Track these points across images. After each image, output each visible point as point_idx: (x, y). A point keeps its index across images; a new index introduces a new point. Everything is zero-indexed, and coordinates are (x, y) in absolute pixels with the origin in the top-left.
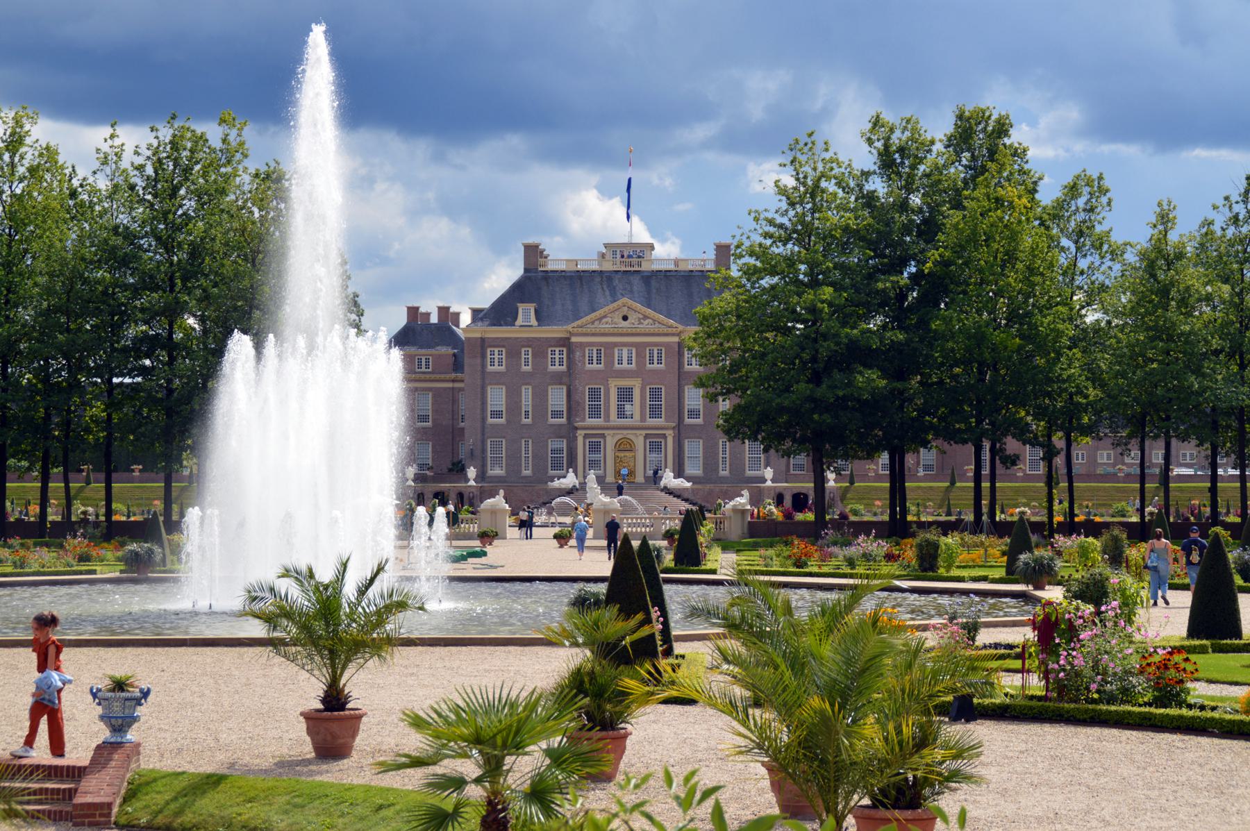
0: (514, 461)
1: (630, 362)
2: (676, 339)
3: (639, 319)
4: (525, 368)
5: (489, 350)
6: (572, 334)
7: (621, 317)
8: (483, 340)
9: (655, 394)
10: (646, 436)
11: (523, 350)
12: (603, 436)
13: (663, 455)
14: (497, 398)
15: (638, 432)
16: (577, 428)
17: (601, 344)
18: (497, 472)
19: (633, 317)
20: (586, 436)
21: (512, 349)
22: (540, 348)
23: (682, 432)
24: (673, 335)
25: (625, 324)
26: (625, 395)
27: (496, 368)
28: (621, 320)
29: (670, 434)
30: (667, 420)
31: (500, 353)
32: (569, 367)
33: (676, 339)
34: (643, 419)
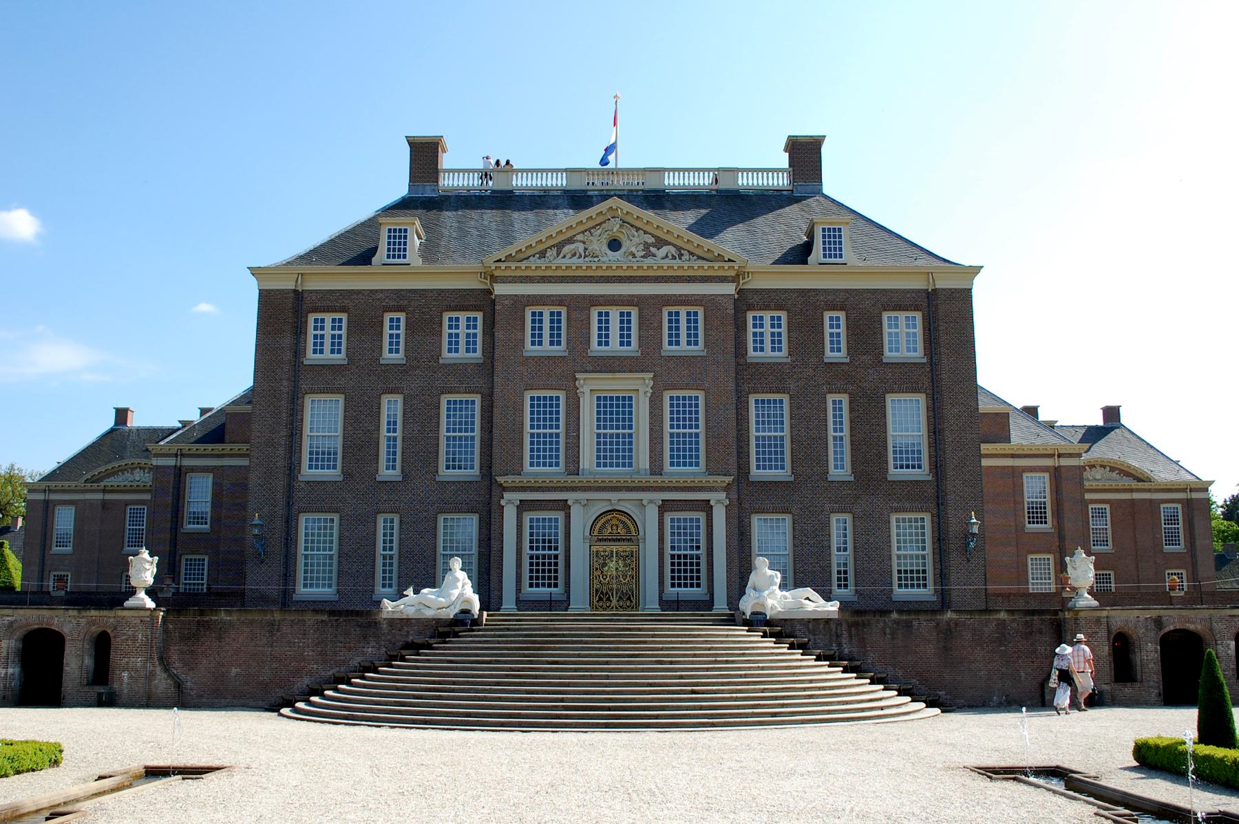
1: (625, 340)
2: (729, 289)
3: (647, 246)
4: (388, 357)
5: (312, 317)
6: (494, 279)
7: (605, 242)
8: (298, 295)
9: (684, 413)
10: (665, 507)
11: (387, 317)
12: (564, 506)
13: (702, 552)
15: (645, 496)
16: (505, 489)
17: (560, 300)
20: (523, 506)
27: (327, 356)
28: (605, 248)
30: (710, 471)
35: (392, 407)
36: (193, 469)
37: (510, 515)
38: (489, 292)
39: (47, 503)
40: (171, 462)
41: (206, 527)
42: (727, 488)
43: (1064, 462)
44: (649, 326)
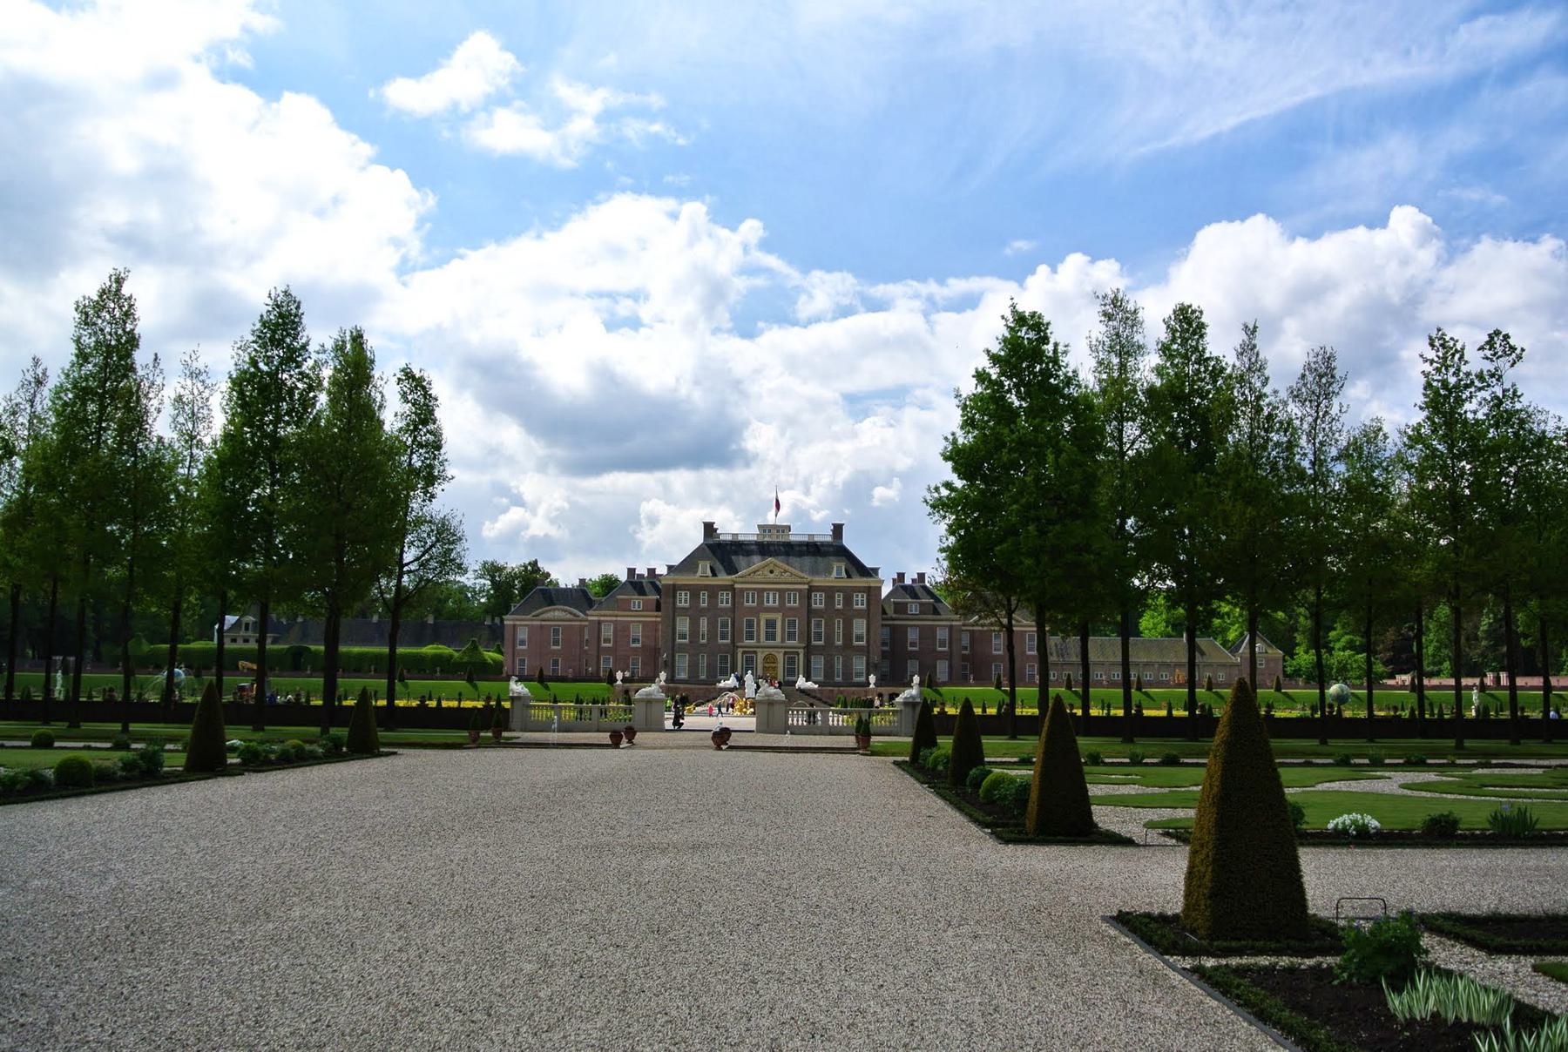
0: (694, 667)
2: (806, 587)
6: (735, 582)
8: (674, 585)
9: (791, 624)
10: (785, 653)
12: (755, 652)
14: (683, 625)
17: (755, 589)
18: (683, 676)
19: (776, 572)
20: (744, 653)
21: (695, 591)
22: (713, 591)
23: (809, 650)
24: (804, 584)
25: (772, 575)
26: (771, 624)
27: (683, 605)
29: (801, 651)
31: (686, 595)
32: (734, 604)
33: (806, 587)
34: (783, 641)
35: (704, 623)
36: (604, 621)
37: (740, 655)
38: (732, 585)
39: (514, 625)
40: (596, 618)
41: (610, 645)
42: (804, 648)
43: (954, 623)
44: (782, 598)
